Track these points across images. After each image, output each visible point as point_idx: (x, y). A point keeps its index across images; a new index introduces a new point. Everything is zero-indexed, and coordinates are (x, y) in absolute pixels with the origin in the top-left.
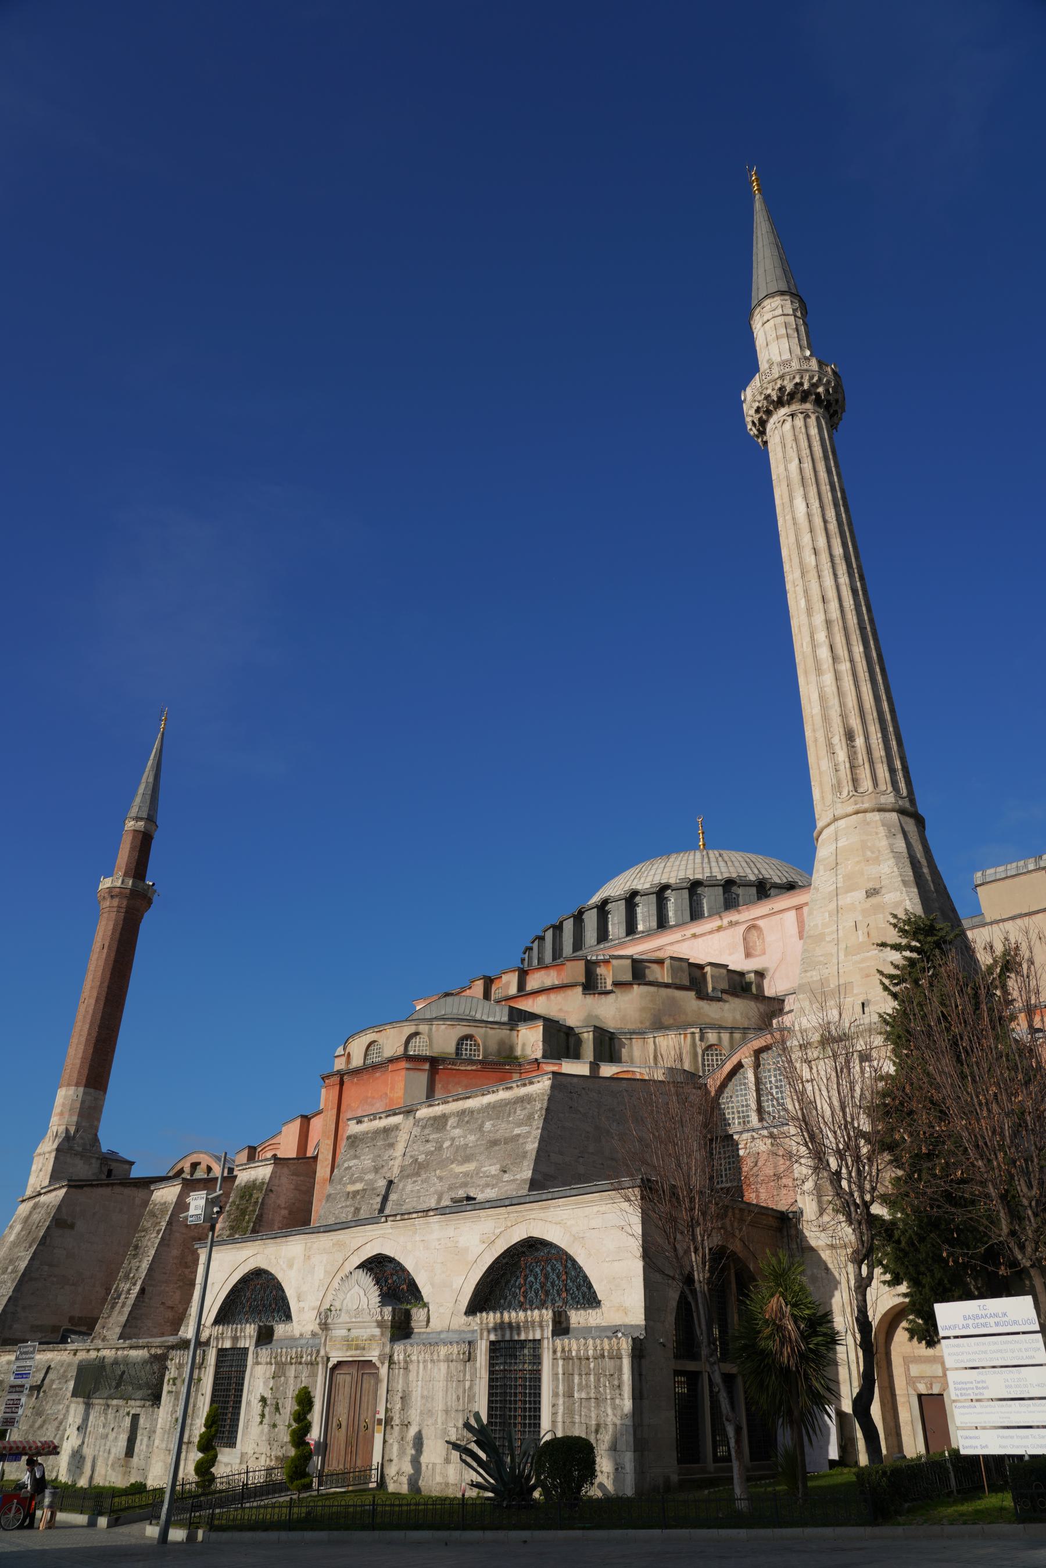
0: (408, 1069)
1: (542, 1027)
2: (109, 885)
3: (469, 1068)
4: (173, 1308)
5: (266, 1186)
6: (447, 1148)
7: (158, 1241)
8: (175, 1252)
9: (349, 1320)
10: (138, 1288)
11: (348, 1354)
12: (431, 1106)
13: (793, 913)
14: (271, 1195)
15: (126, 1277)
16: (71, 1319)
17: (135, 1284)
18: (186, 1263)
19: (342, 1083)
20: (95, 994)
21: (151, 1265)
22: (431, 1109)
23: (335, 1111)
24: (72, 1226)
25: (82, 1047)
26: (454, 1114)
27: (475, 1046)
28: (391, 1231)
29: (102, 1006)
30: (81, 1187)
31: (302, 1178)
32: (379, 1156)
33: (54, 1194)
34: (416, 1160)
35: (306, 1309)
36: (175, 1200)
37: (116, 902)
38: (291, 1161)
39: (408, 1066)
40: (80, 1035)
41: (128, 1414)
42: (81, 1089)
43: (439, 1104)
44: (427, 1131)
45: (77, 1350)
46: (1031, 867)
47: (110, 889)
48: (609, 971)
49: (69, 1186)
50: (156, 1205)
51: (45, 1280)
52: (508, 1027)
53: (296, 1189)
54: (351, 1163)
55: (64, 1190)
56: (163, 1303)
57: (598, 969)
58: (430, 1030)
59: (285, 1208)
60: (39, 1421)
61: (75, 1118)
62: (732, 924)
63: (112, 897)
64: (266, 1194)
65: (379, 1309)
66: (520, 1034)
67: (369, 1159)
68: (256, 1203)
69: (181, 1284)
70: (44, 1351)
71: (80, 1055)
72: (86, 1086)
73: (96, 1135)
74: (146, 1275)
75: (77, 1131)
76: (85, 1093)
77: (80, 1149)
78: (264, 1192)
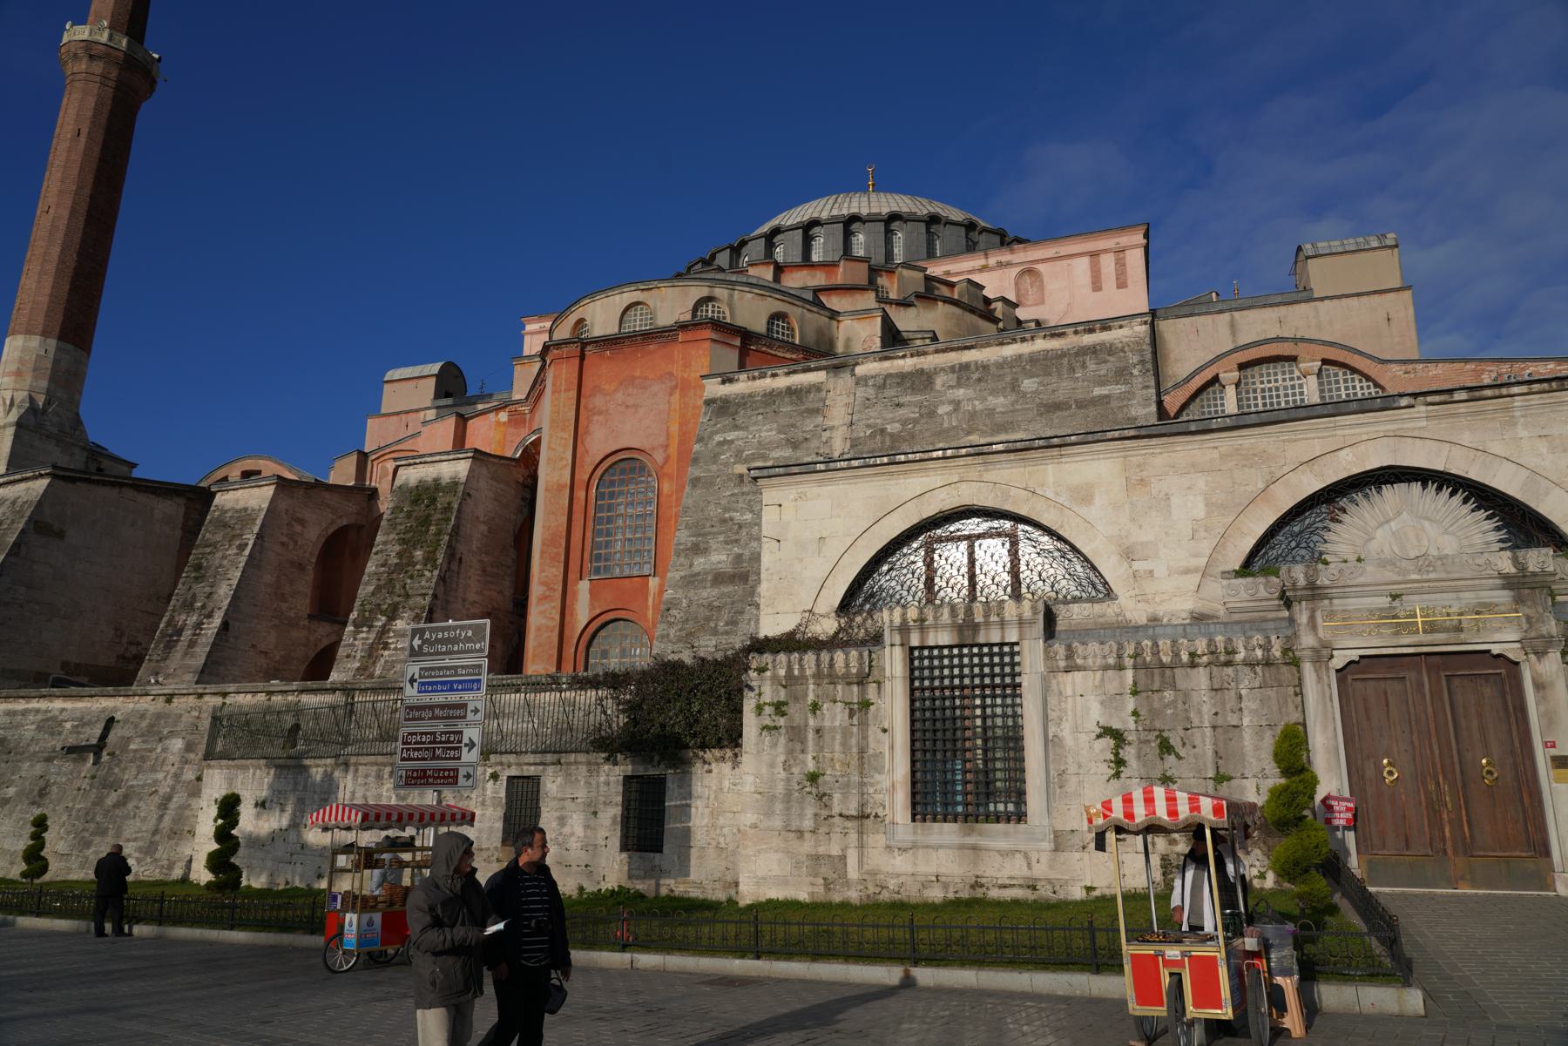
0: (714, 341)
1: (879, 319)
2: (85, 36)
3: (788, 356)
4: (266, 653)
5: (462, 487)
6: (949, 414)
7: (243, 560)
8: (268, 578)
9: (1400, 578)
10: (217, 621)
11: (1394, 642)
12: (887, 358)
13: (1086, 260)
14: (469, 501)
15: (188, 606)
16: (65, 665)
17: (210, 616)
18: (283, 594)
19: (582, 357)
20: (69, 203)
21: (236, 590)
22: (887, 364)
23: (574, 394)
24: (61, 535)
25: (48, 281)
26: (942, 369)
27: (788, 330)
28: (1423, 423)
29: (81, 223)
30: (73, 480)
31: (502, 486)
32: (793, 426)
33: (23, 486)
34: (883, 431)
35: (1160, 571)
36: (265, 505)
37: (98, 67)
38: (492, 459)
39: (714, 336)
40: (45, 261)
41: (495, 777)
42: (52, 343)
43: (904, 357)
44: (889, 393)
45: (172, 695)
46: (1375, 244)
47: (88, 45)
48: (892, 283)
49: (53, 476)
50: (226, 512)
51: (21, 606)
52: (828, 314)
53: (495, 500)
54: (731, 436)
55: (45, 482)
56: (253, 646)
57: (879, 278)
58: (731, 296)
59: (484, 523)
60: (113, 797)
61: (44, 384)
62: (1000, 265)
63: (91, 57)
64: (463, 499)
65: (1508, 554)
66: (842, 325)
67: (771, 430)
68: (448, 508)
69: (276, 622)
70: (92, 696)
71: (47, 291)
72: (60, 339)
73: (78, 415)
74: (230, 604)
75: (48, 402)
76: (58, 349)
77: (55, 430)
78: (460, 494)
